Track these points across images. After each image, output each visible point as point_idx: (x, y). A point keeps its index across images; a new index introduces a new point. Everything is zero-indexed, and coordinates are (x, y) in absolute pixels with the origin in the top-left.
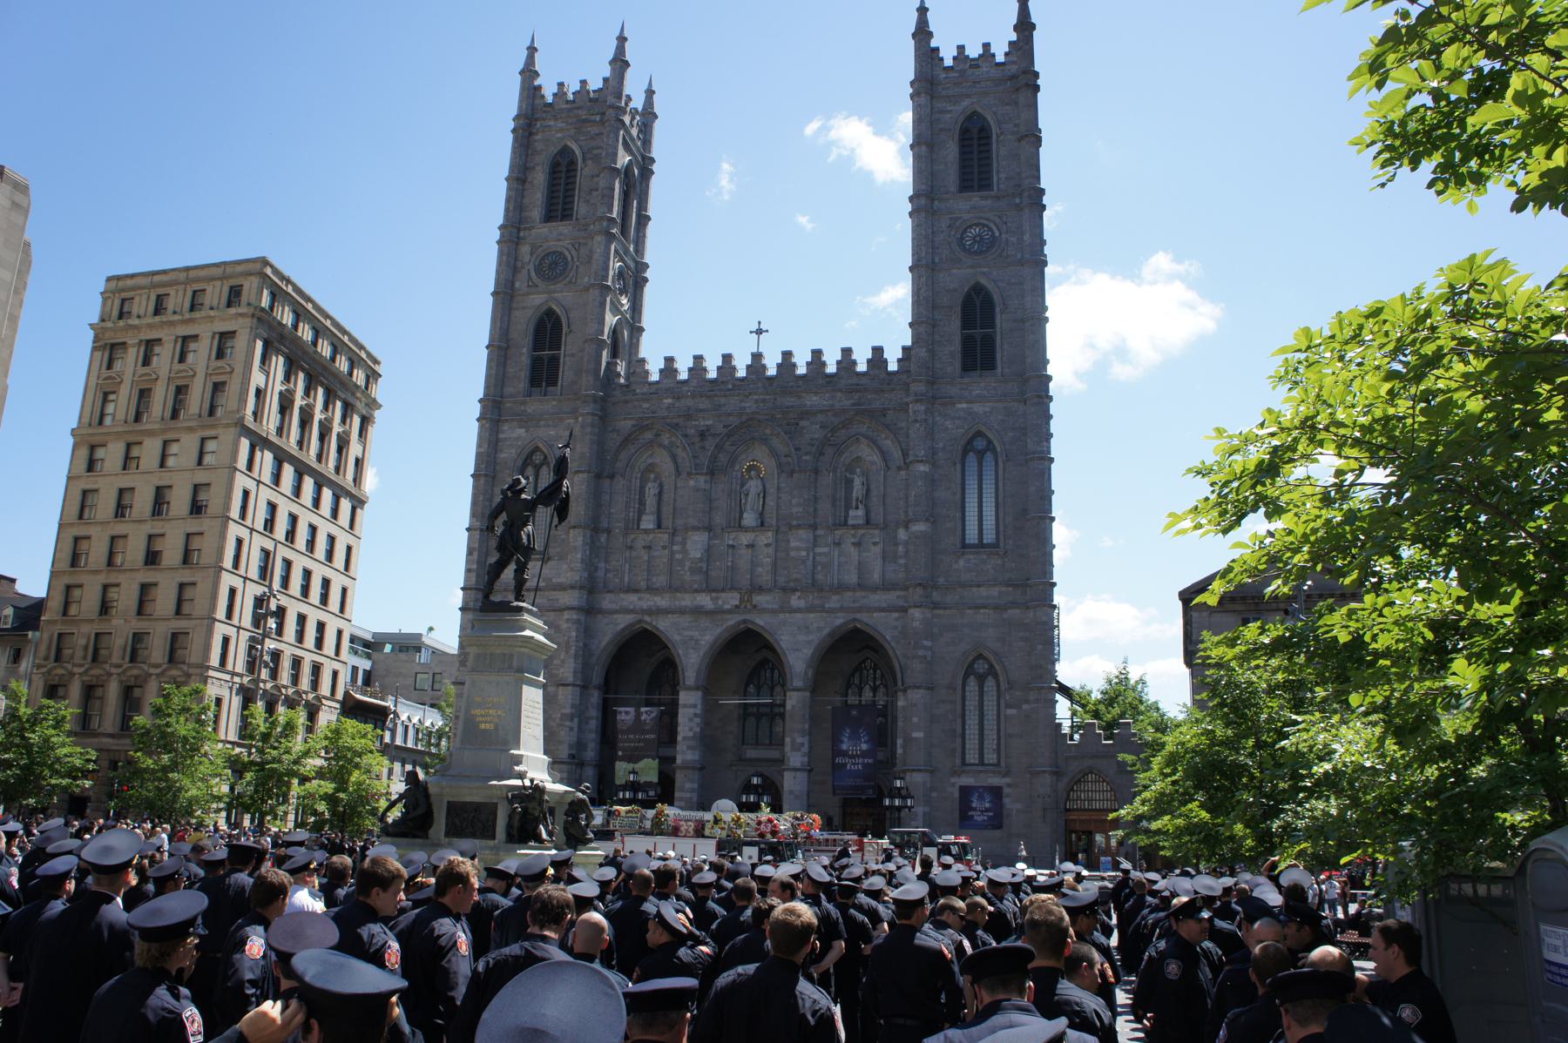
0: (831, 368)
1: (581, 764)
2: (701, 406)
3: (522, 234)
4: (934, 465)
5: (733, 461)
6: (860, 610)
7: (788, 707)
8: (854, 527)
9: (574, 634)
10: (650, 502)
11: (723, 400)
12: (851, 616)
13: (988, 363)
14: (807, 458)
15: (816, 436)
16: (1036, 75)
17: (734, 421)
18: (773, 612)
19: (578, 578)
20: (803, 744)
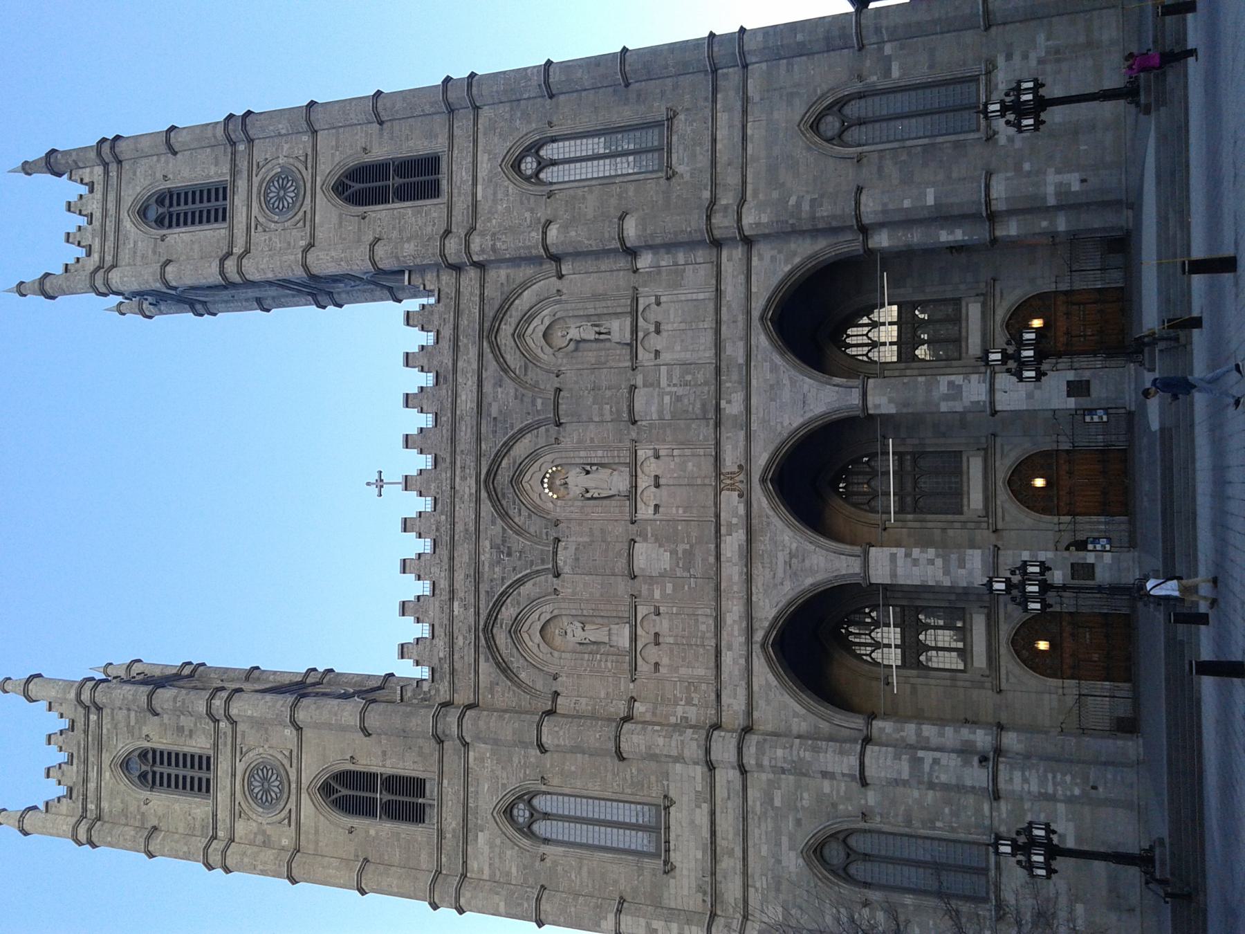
0: (427, 380)
1: (998, 751)
2: (466, 558)
3: (221, 834)
4: (548, 223)
5: (536, 511)
6: (748, 313)
7: (892, 410)
8: (635, 330)
9: (780, 752)
10: (593, 634)
11: (459, 527)
12: (756, 323)
13: (430, 164)
14: (539, 401)
15: (512, 392)
16: (104, 140)
17: (487, 507)
18: (748, 438)
19: (694, 744)
20: (951, 384)
